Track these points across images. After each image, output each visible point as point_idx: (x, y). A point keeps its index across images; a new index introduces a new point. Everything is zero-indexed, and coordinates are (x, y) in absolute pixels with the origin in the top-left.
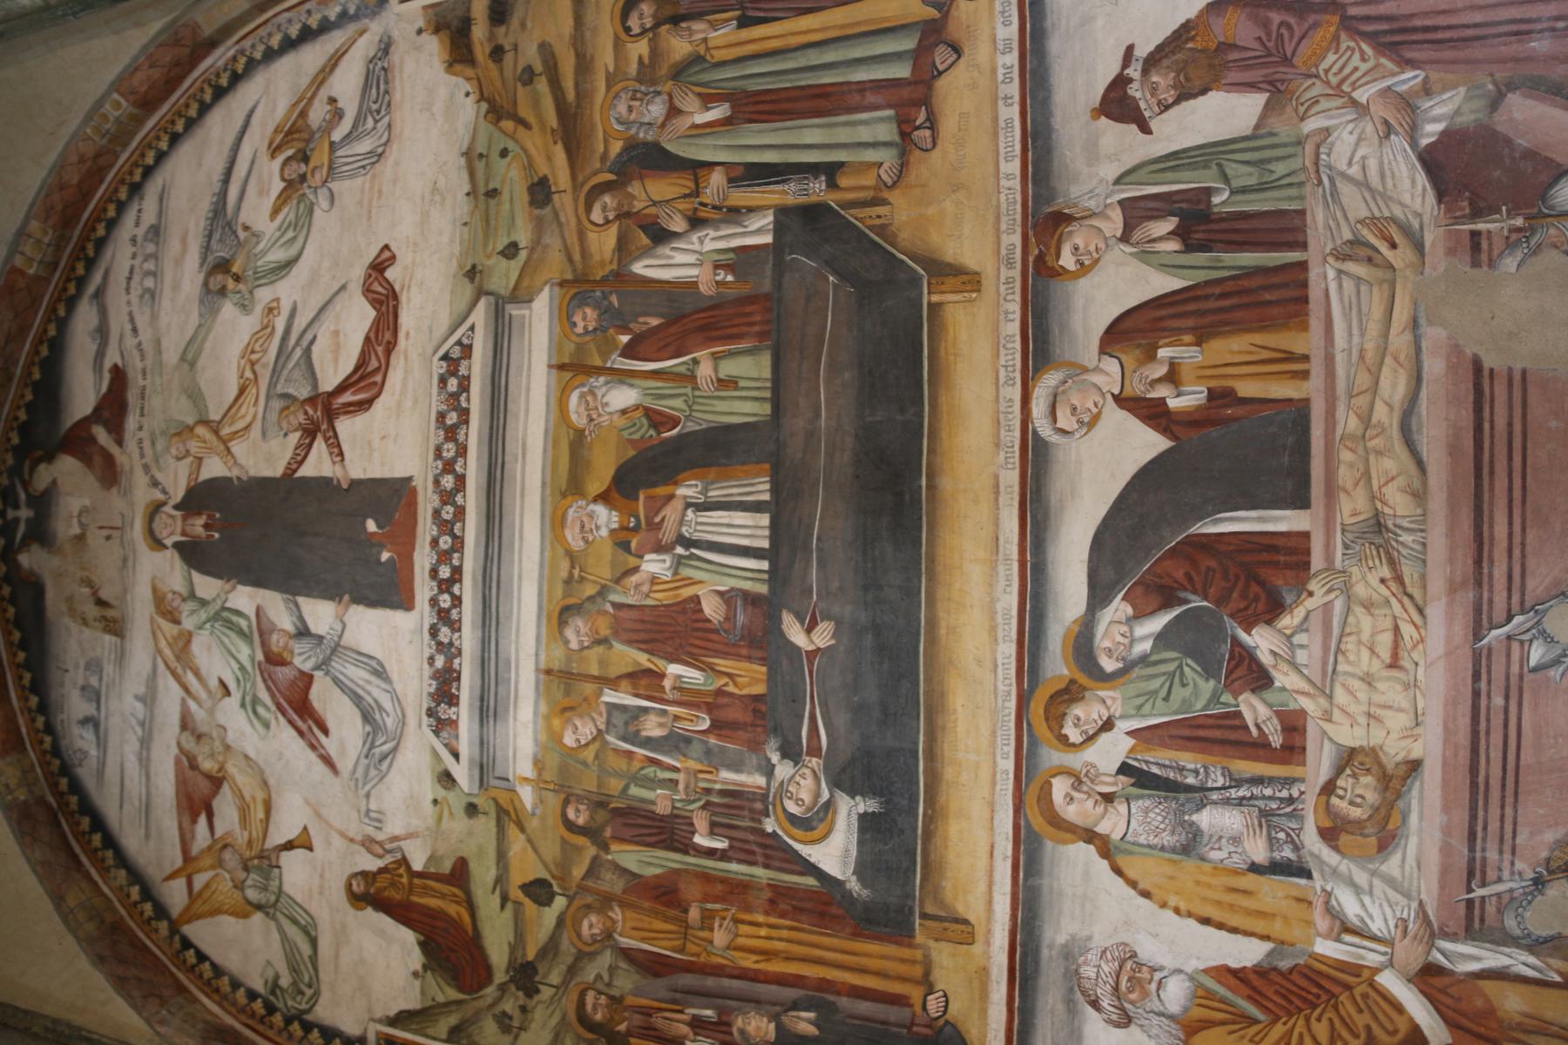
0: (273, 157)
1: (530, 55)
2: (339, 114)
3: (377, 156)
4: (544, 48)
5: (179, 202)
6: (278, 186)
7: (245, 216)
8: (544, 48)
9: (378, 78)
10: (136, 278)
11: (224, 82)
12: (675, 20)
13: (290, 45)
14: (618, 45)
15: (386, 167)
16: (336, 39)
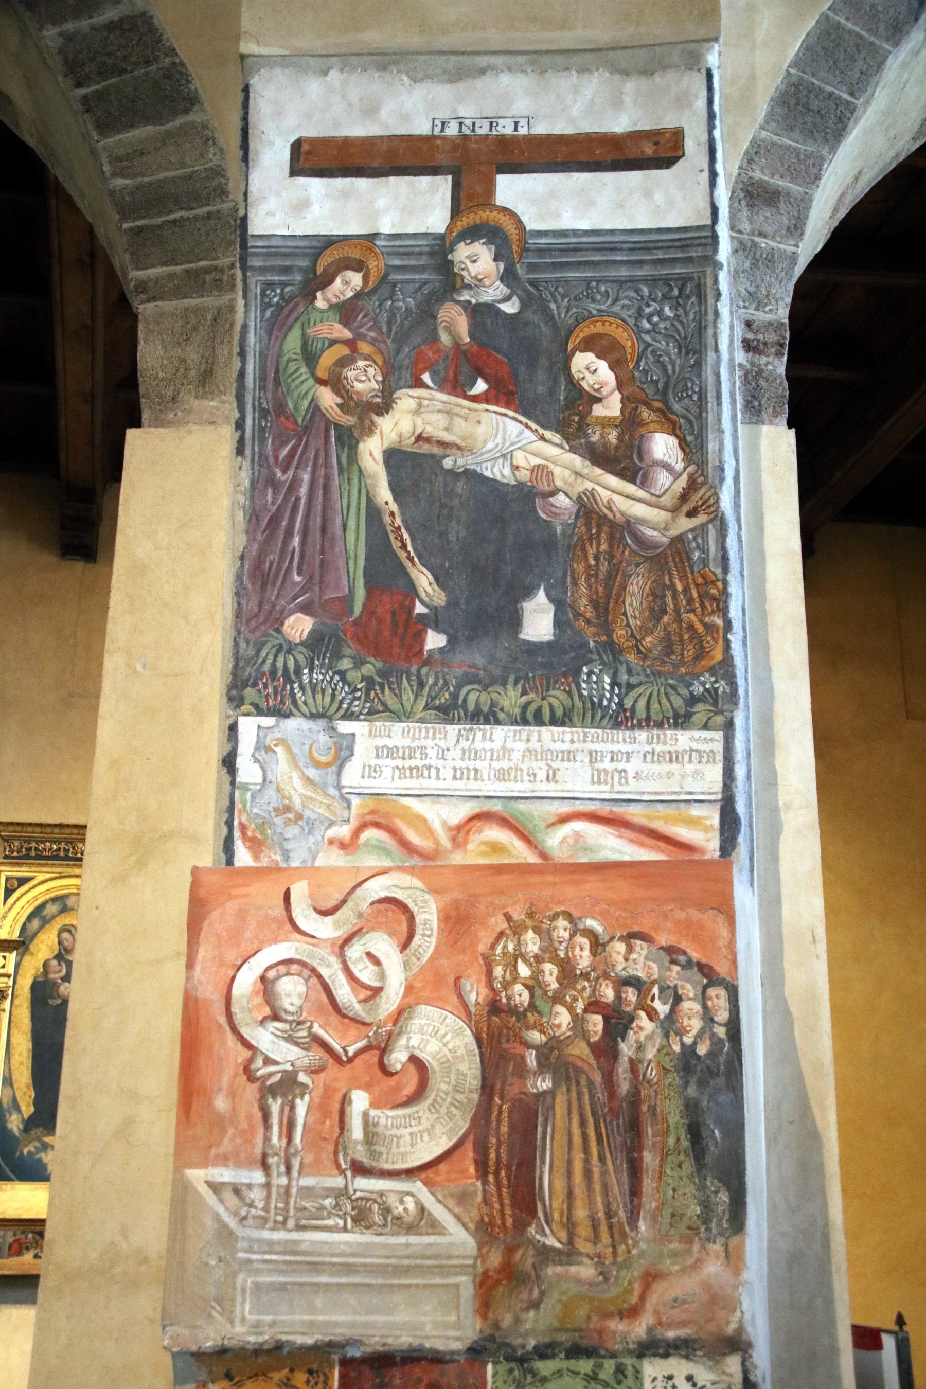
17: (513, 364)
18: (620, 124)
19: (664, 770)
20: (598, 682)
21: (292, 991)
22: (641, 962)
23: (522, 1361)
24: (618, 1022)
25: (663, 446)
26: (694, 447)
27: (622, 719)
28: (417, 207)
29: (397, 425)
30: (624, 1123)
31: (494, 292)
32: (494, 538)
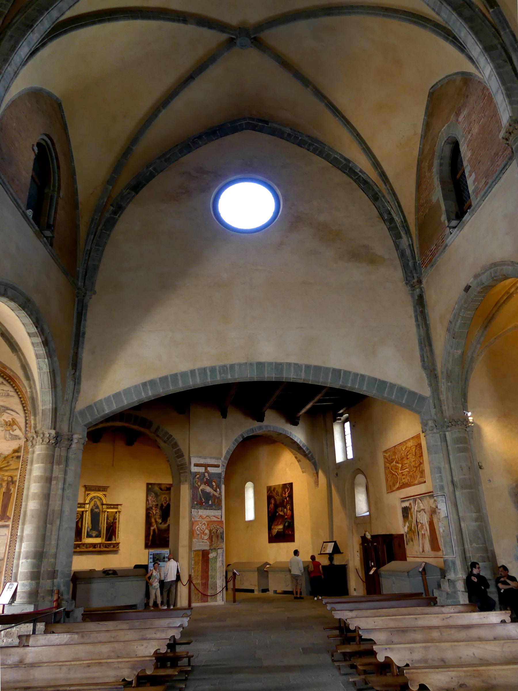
0: (12, 419)
1: (11, 462)
2: (13, 431)
3: (5, 439)
4: (11, 464)
5: (11, 400)
6: (7, 420)
7: (5, 414)
8: (11, 464)
9: (17, 437)
10: (2, 391)
11: (25, 408)
12: (7, 484)
13: (26, 420)
14: (7, 476)
15: (4, 441)
16: (23, 429)
17: (208, 483)
18: (216, 464)
19: (217, 513)
20: (214, 507)
21: (199, 529)
22: (218, 527)
23: (211, 550)
24: (217, 531)
25: (218, 490)
26: (220, 490)
27: (215, 510)
28: (202, 470)
29: (201, 488)
30: (218, 537)
31: (207, 477)
32: (207, 496)
